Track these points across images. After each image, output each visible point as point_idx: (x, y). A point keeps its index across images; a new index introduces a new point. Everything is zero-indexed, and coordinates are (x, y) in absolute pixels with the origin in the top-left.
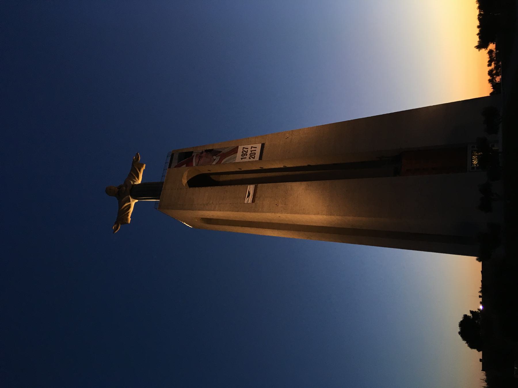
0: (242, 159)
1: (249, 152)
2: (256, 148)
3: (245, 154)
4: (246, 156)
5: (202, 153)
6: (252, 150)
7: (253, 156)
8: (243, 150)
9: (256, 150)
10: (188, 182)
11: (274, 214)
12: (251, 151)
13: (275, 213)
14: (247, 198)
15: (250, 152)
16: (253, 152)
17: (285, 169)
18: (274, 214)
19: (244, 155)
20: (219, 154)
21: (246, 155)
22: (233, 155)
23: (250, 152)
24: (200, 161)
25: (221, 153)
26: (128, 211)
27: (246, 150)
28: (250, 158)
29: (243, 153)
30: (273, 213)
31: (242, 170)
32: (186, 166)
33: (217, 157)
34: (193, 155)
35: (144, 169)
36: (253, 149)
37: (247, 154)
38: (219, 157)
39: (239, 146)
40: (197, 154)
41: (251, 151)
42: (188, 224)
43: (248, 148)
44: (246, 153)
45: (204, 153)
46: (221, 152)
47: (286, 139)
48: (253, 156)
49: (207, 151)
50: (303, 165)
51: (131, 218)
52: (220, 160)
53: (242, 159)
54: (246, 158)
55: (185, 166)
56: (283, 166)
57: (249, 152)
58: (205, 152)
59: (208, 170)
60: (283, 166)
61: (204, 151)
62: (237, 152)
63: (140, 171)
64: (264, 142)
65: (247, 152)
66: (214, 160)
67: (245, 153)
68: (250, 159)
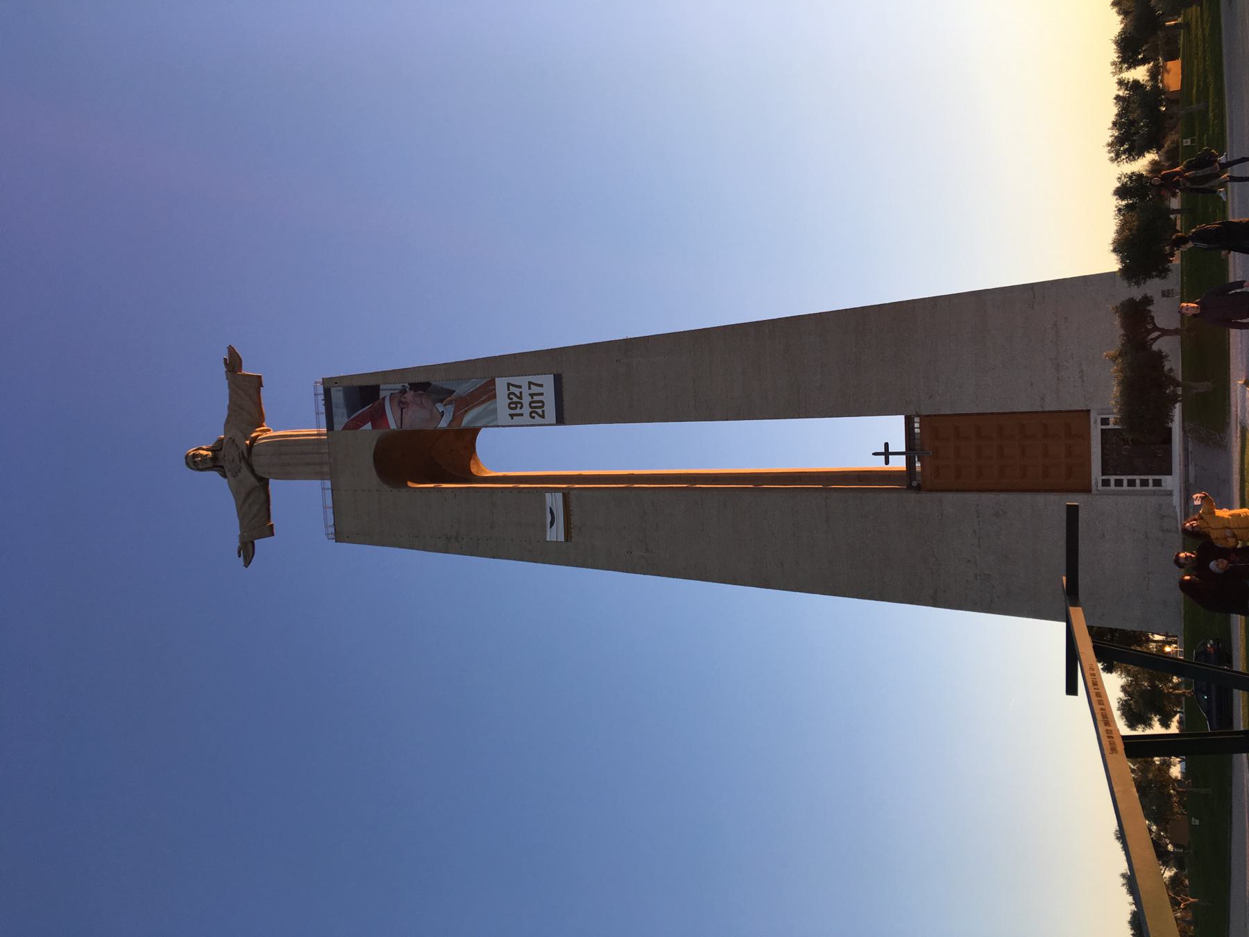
0: (512, 416)
1: (526, 400)
2: (541, 386)
3: (516, 403)
4: (521, 408)
5: (403, 391)
6: (531, 392)
7: (539, 411)
8: (509, 390)
9: (542, 394)
12: (530, 394)
14: (551, 527)
15: (530, 399)
16: (536, 398)
19: (514, 406)
20: (449, 399)
21: (519, 405)
22: (486, 404)
23: (530, 399)
24: (404, 415)
25: (454, 396)
27: (517, 391)
28: (533, 415)
29: (512, 399)
32: (374, 426)
33: (445, 405)
34: (381, 396)
36: (535, 389)
37: (522, 404)
38: (451, 408)
39: (497, 379)
40: (392, 394)
41: (530, 394)
43: (520, 387)
44: (518, 400)
45: (410, 395)
46: (454, 392)
48: (539, 411)
49: (415, 387)
52: (457, 417)
53: (512, 419)
54: (522, 415)
55: (370, 428)
57: (526, 400)
58: (410, 389)
61: (407, 385)
62: (494, 397)
64: (560, 373)
65: (520, 398)
66: (443, 416)
67: (515, 399)
68: (533, 418)
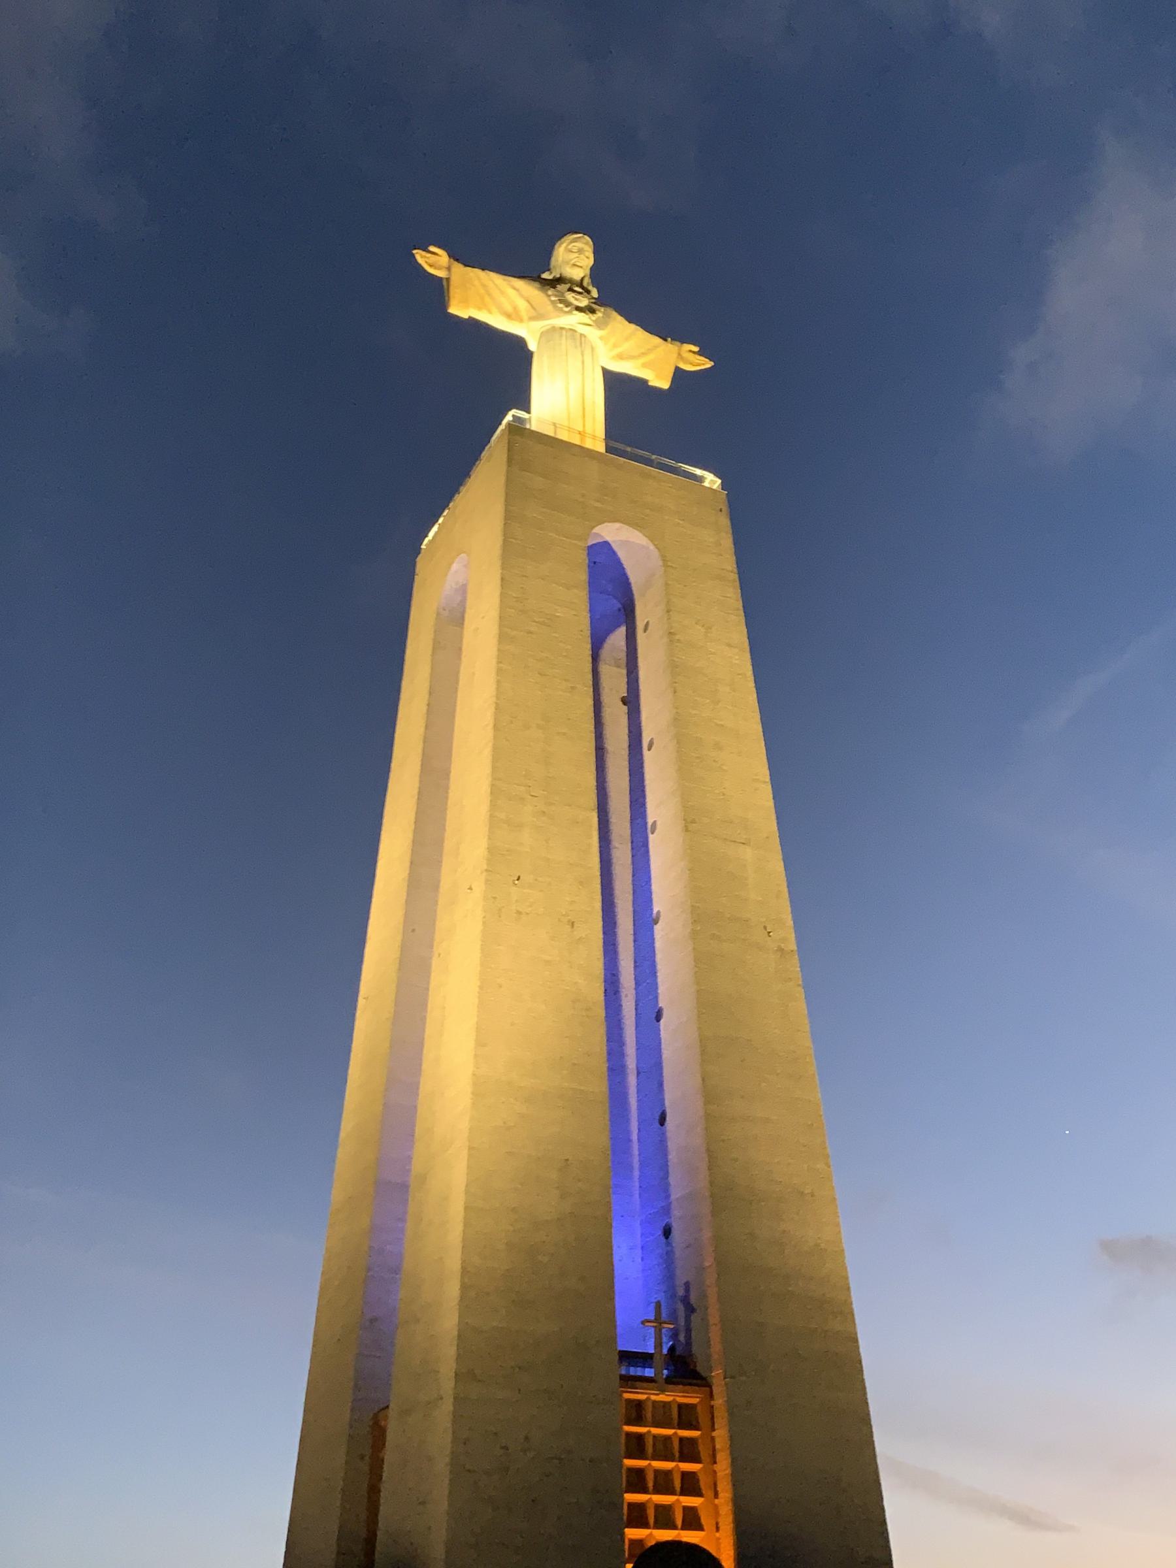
10: (606, 544)
11: (485, 867)
13: (486, 870)
17: (645, 920)
18: (485, 867)
26: (494, 310)
30: (488, 864)
31: (647, 755)
35: (650, 384)
42: (436, 533)
47: (765, 928)
50: (661, 990)
51: (470, 317)
56: (659, 912)
59: (648, 623)
60: (659, 912)
63: (645, 365)
